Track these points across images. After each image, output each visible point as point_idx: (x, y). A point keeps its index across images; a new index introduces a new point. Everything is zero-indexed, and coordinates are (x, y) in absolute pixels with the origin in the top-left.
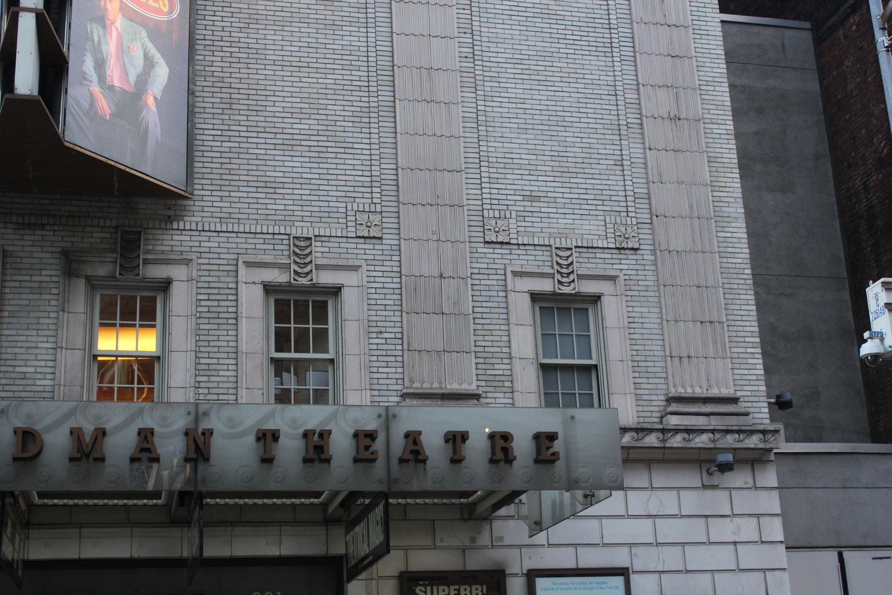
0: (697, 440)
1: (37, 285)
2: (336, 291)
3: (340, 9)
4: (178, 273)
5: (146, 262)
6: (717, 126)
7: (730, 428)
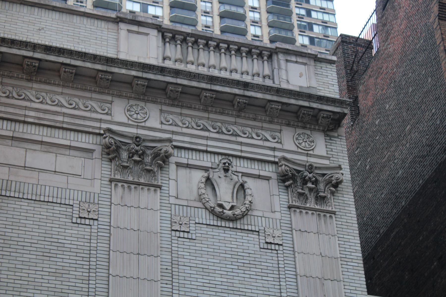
3: (67, 280)
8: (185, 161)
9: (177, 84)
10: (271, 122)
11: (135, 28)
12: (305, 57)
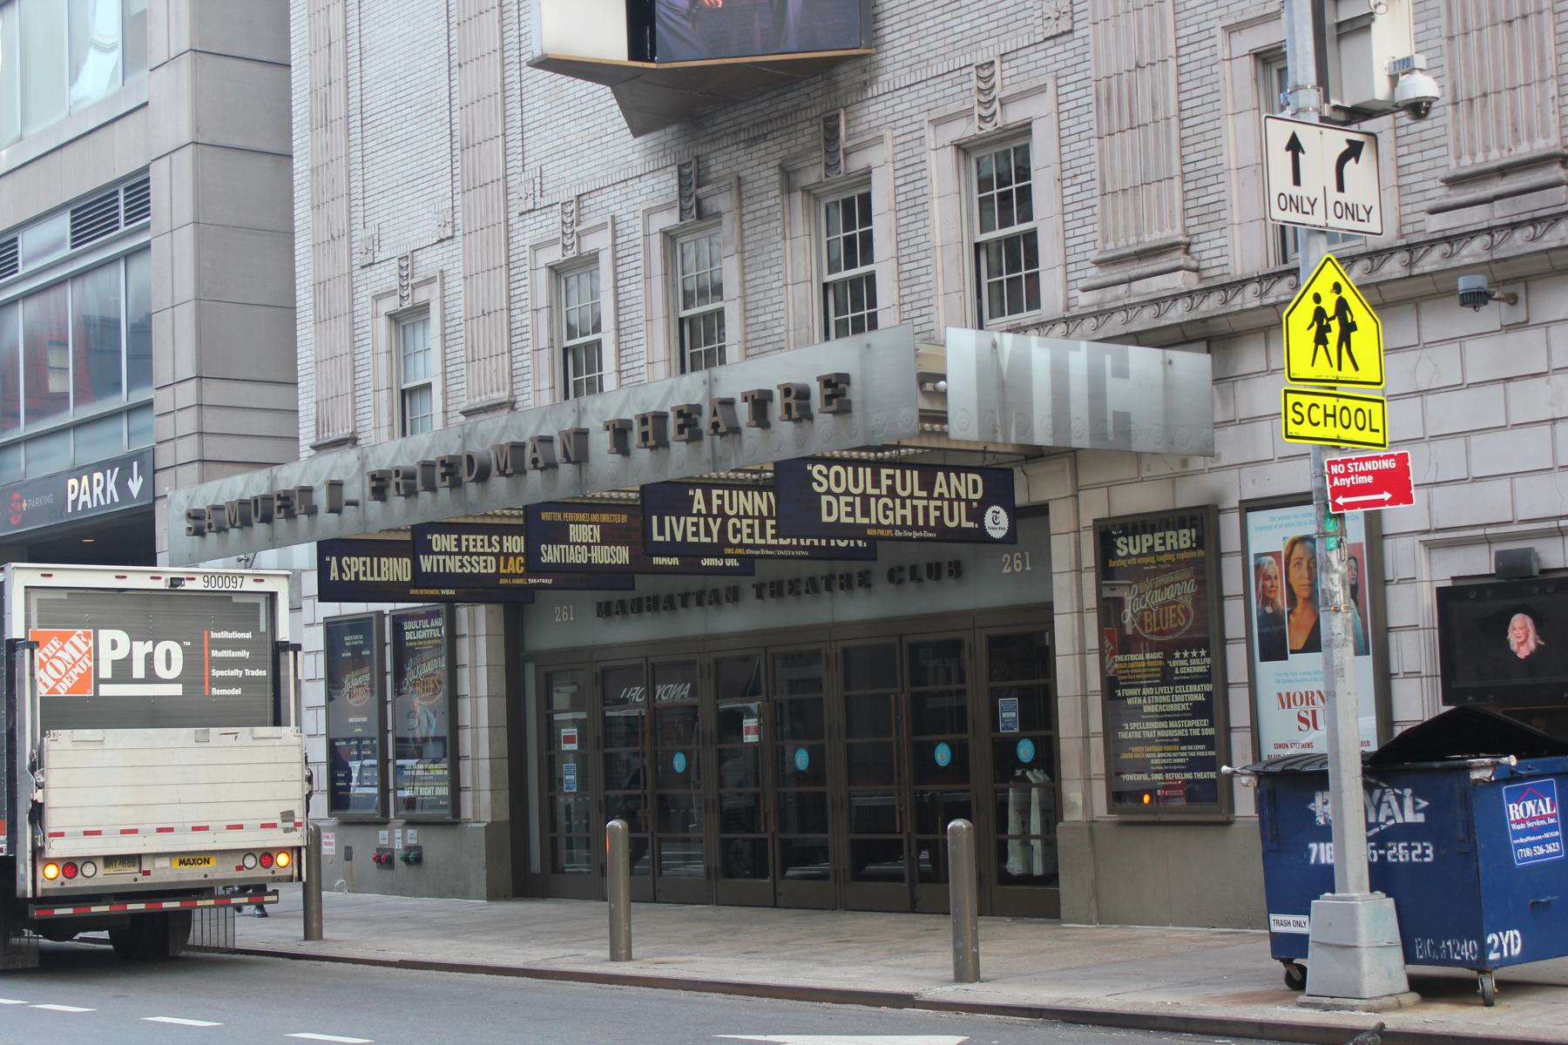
0: (1465, 252)
1: (765, 212)
2: (1025, 129)
4: (875, 157)
5: (846, 154)
7: (1516, 219)
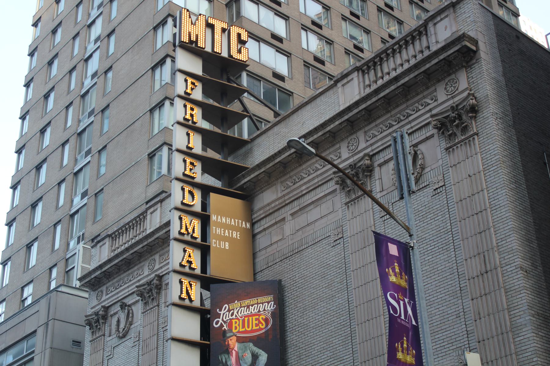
6: (509, 266)
8: (382, 160)
9: (360, 111)
10: (428, 88)
11: (345, 81)
12: (446, 9)
